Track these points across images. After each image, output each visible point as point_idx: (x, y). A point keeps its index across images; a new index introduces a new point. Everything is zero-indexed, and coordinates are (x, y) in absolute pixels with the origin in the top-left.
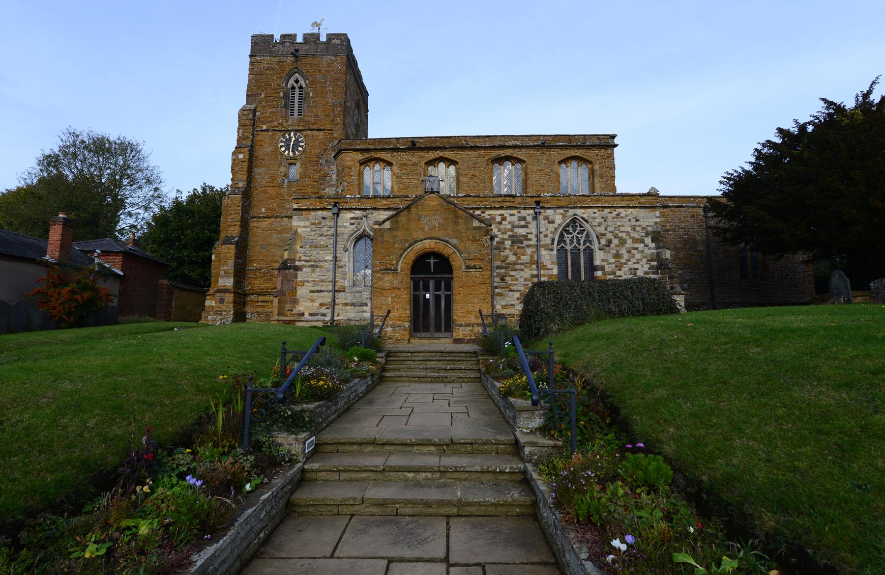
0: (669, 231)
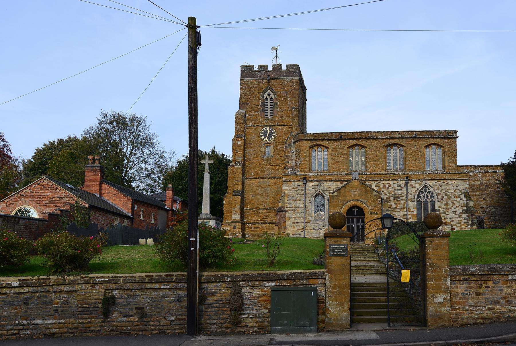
0: (488, 186)
